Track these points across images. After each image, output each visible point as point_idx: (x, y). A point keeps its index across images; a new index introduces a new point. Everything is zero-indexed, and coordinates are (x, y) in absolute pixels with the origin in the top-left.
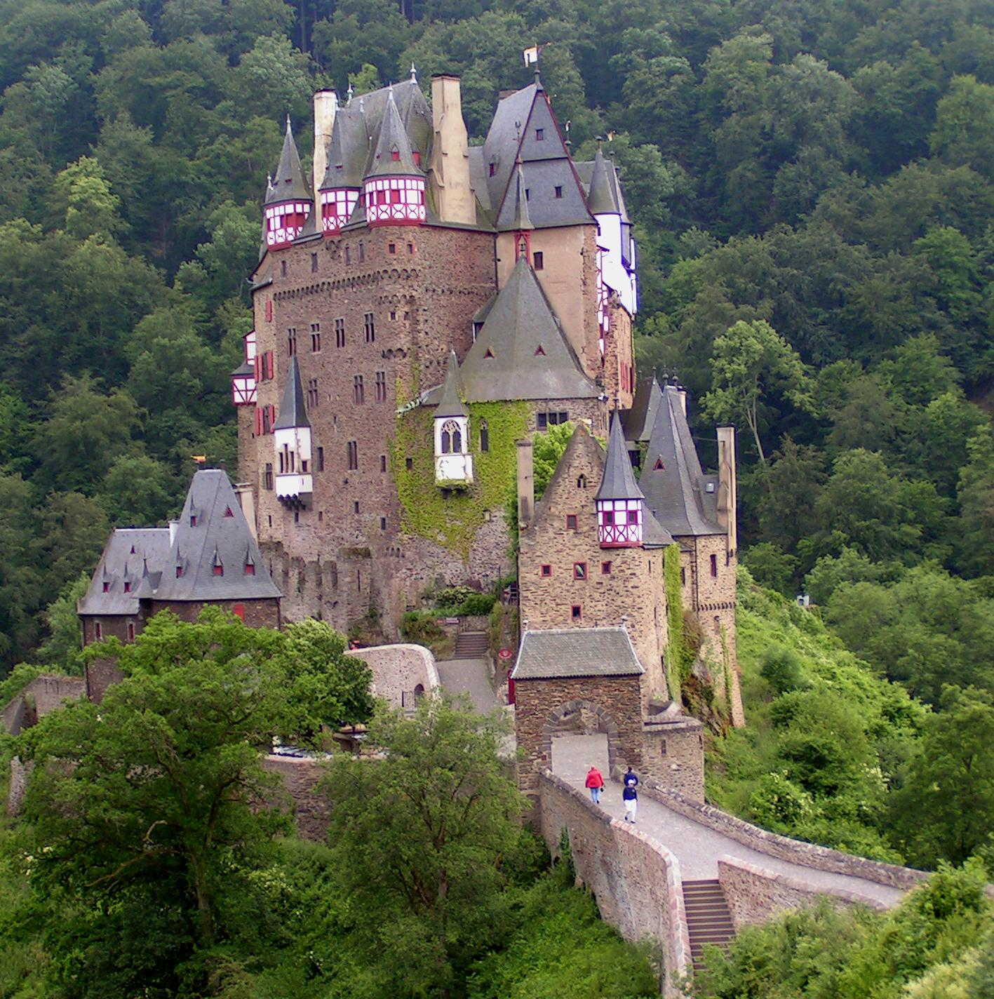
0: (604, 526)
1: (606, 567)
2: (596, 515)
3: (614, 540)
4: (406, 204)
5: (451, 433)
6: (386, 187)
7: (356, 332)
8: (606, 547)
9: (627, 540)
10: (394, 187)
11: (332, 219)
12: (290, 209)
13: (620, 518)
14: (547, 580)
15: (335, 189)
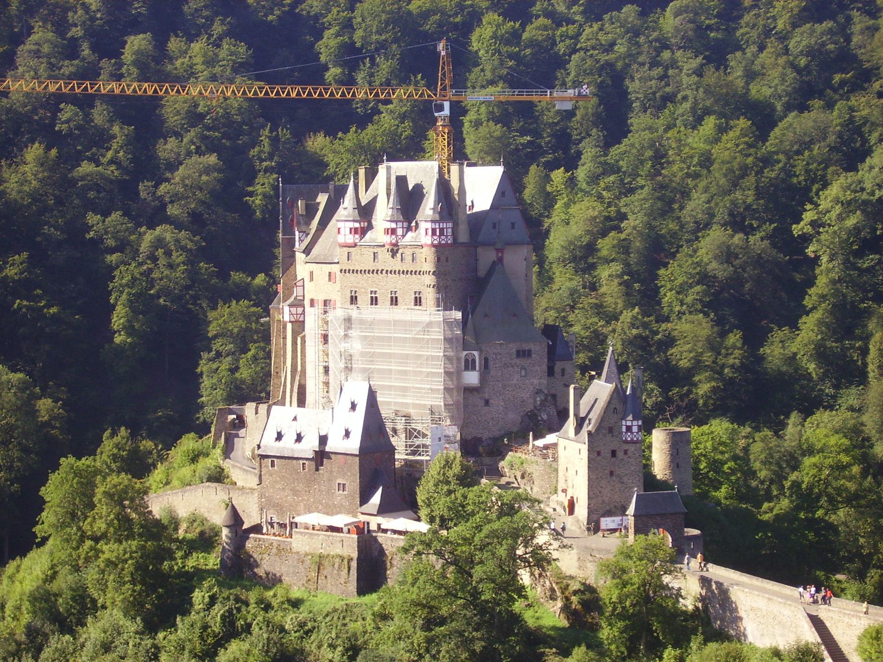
0: (626, 433)
1: (626, 452)
2: (621, 427)
3: (632, 439)
4: (447, 236)
5: (470, 360)
6: (437, 227)
7: (407, 299)
8: (626, 442)
9: (637, 439)
10: (441, 227)
11: (393, 237)
12: (357, 225)
13: (635, 429)
14: (599, 458)
15: (396, 222)
